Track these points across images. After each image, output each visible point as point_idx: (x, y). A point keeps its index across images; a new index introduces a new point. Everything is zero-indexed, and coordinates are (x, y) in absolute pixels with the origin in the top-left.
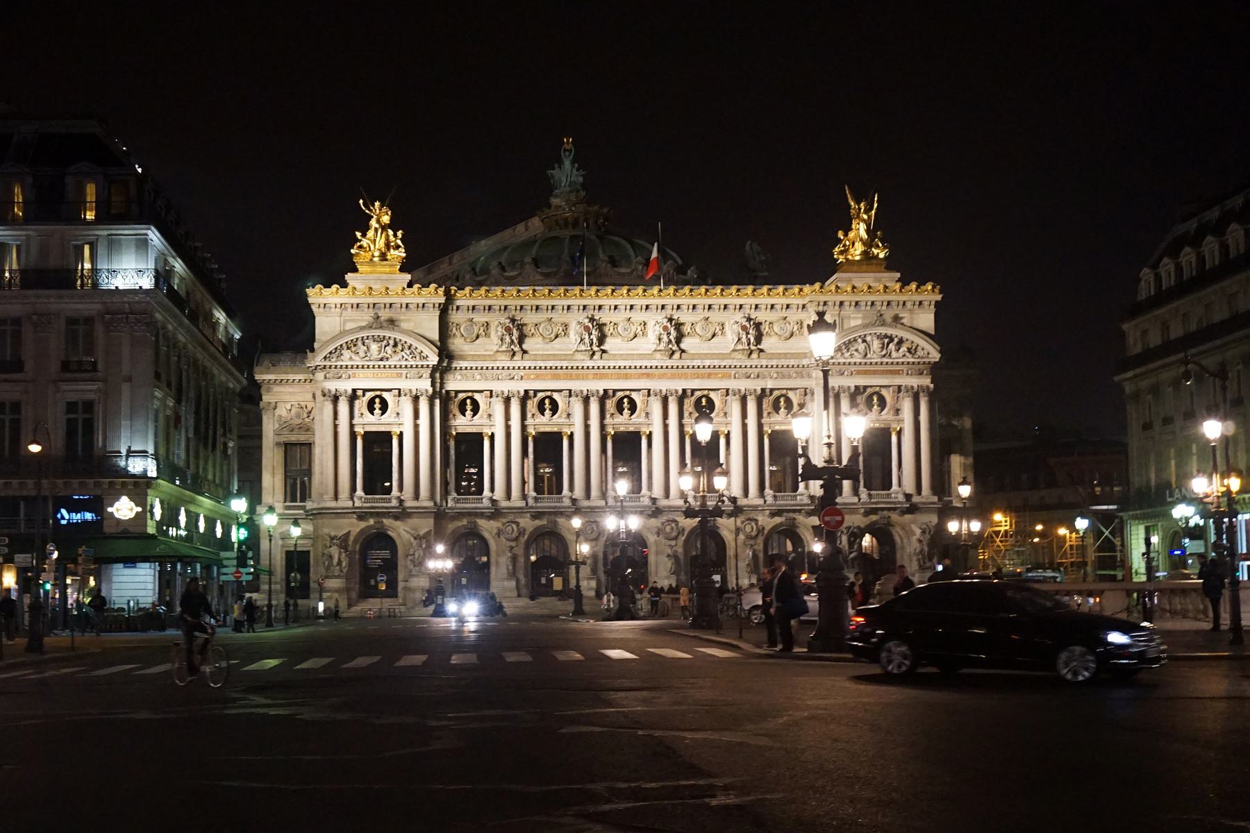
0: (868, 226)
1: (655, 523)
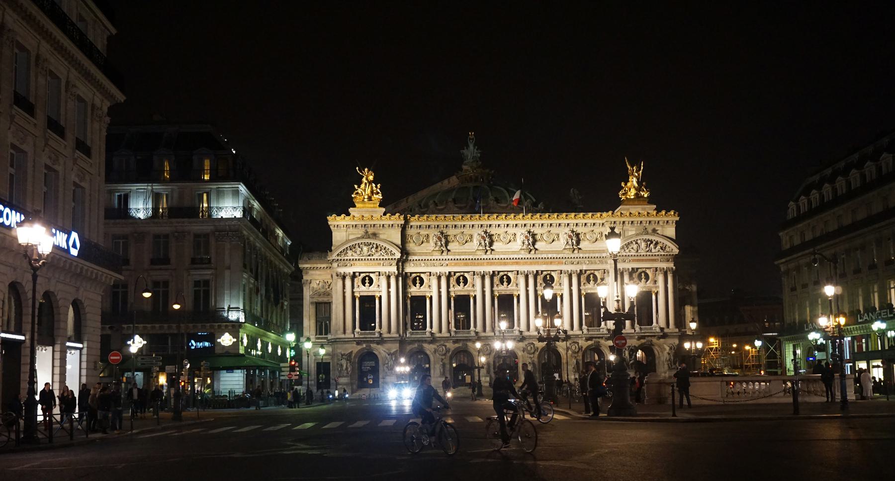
0: (638, 179)
1: (522, 345)
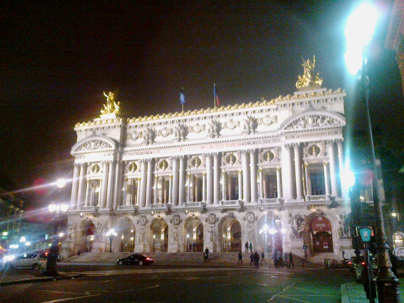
1: (205, 216)
